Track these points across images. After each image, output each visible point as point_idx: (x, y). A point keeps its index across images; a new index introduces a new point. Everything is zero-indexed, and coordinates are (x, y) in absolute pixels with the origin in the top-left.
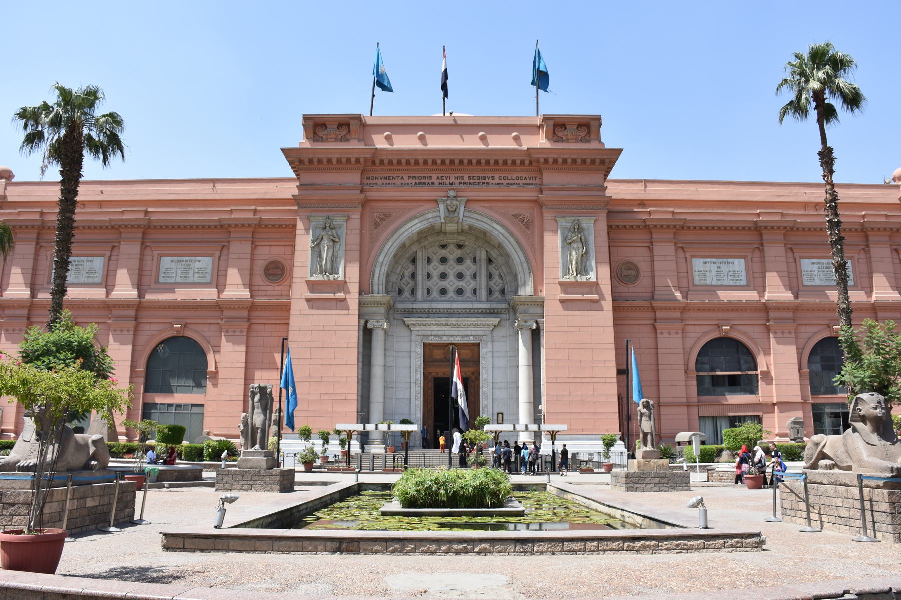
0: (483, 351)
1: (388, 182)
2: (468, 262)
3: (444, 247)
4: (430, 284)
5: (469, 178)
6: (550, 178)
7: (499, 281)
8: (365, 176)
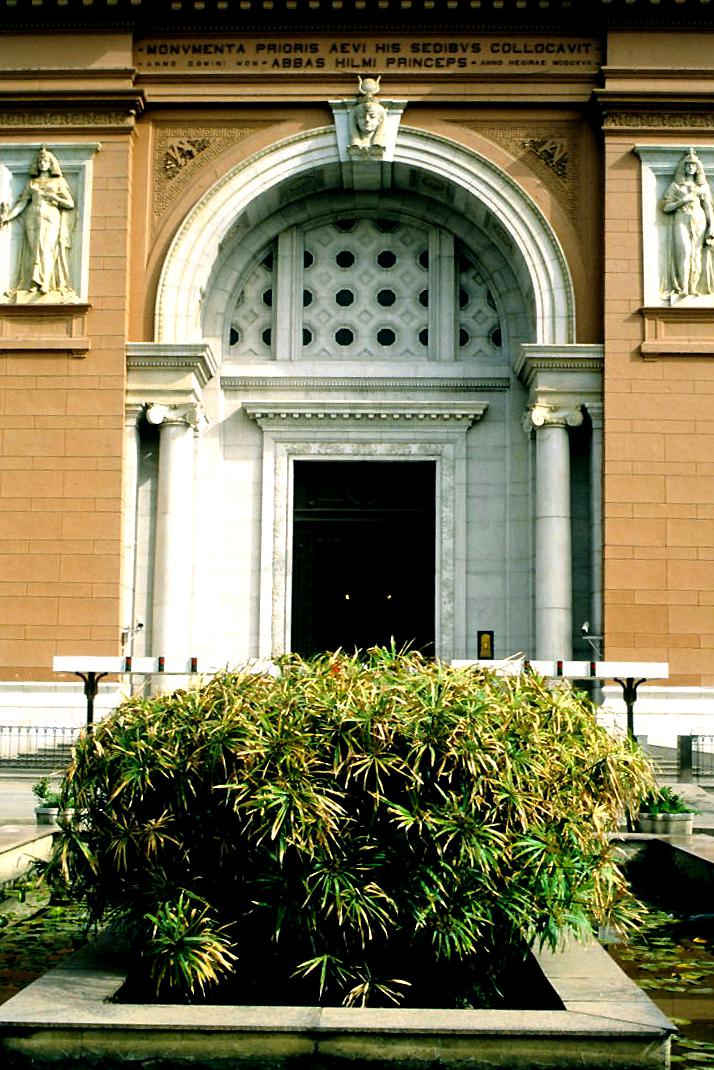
1: (204, 58)
2: (406, 264)
3: (345, 226)
4: (313, 316)
5: (415, 48)
7: (487, 311)
8: (145, 44)
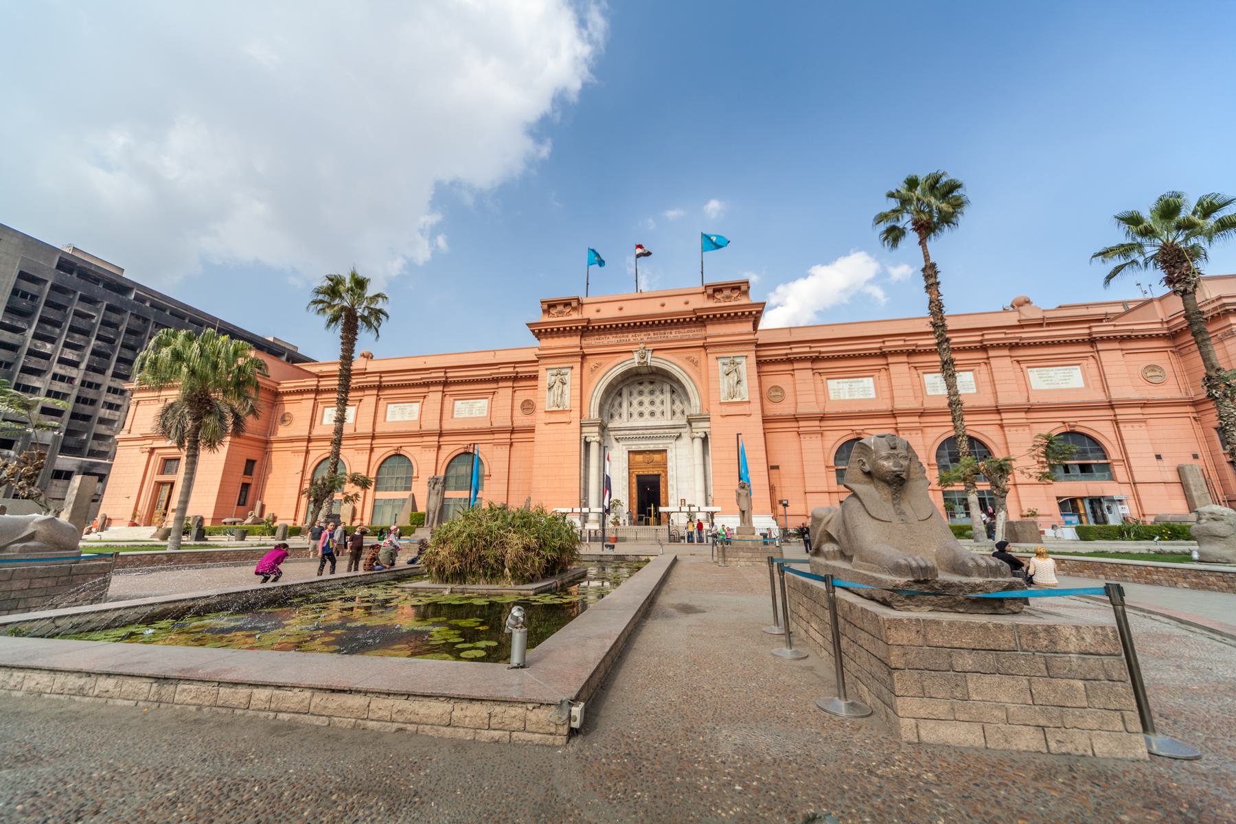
0: (669, 454)
2: (658, 393)
3: (641, 384)
4: (631, 409)
6: (712, 330)
